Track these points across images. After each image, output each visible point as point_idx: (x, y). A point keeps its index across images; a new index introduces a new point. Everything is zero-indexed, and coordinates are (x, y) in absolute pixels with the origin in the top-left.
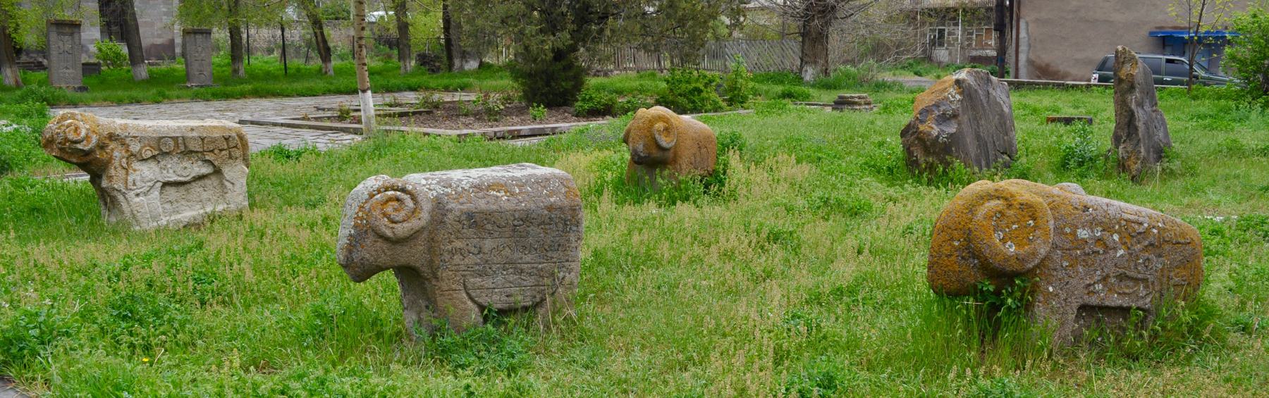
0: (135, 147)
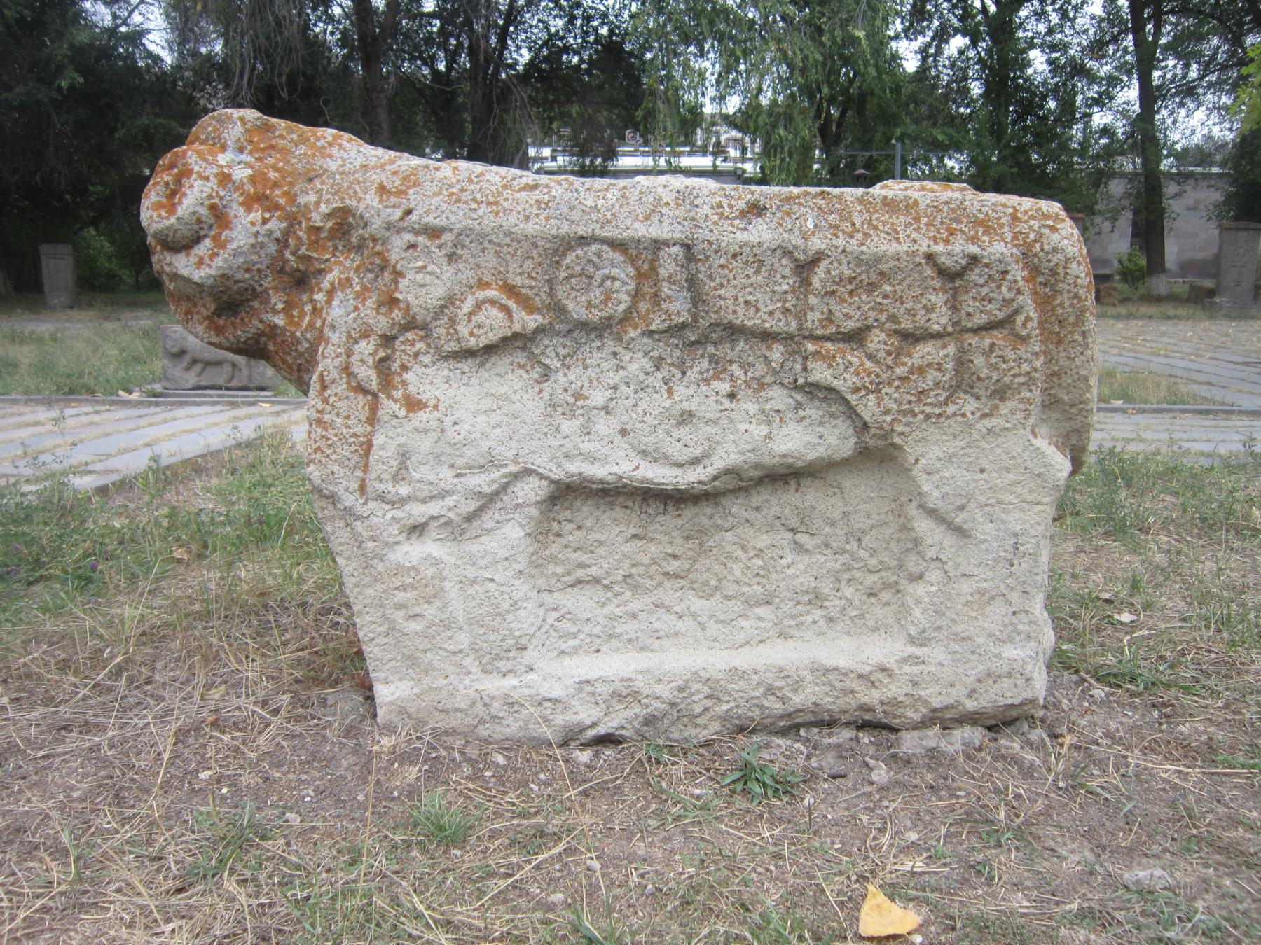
0: (425, 284)
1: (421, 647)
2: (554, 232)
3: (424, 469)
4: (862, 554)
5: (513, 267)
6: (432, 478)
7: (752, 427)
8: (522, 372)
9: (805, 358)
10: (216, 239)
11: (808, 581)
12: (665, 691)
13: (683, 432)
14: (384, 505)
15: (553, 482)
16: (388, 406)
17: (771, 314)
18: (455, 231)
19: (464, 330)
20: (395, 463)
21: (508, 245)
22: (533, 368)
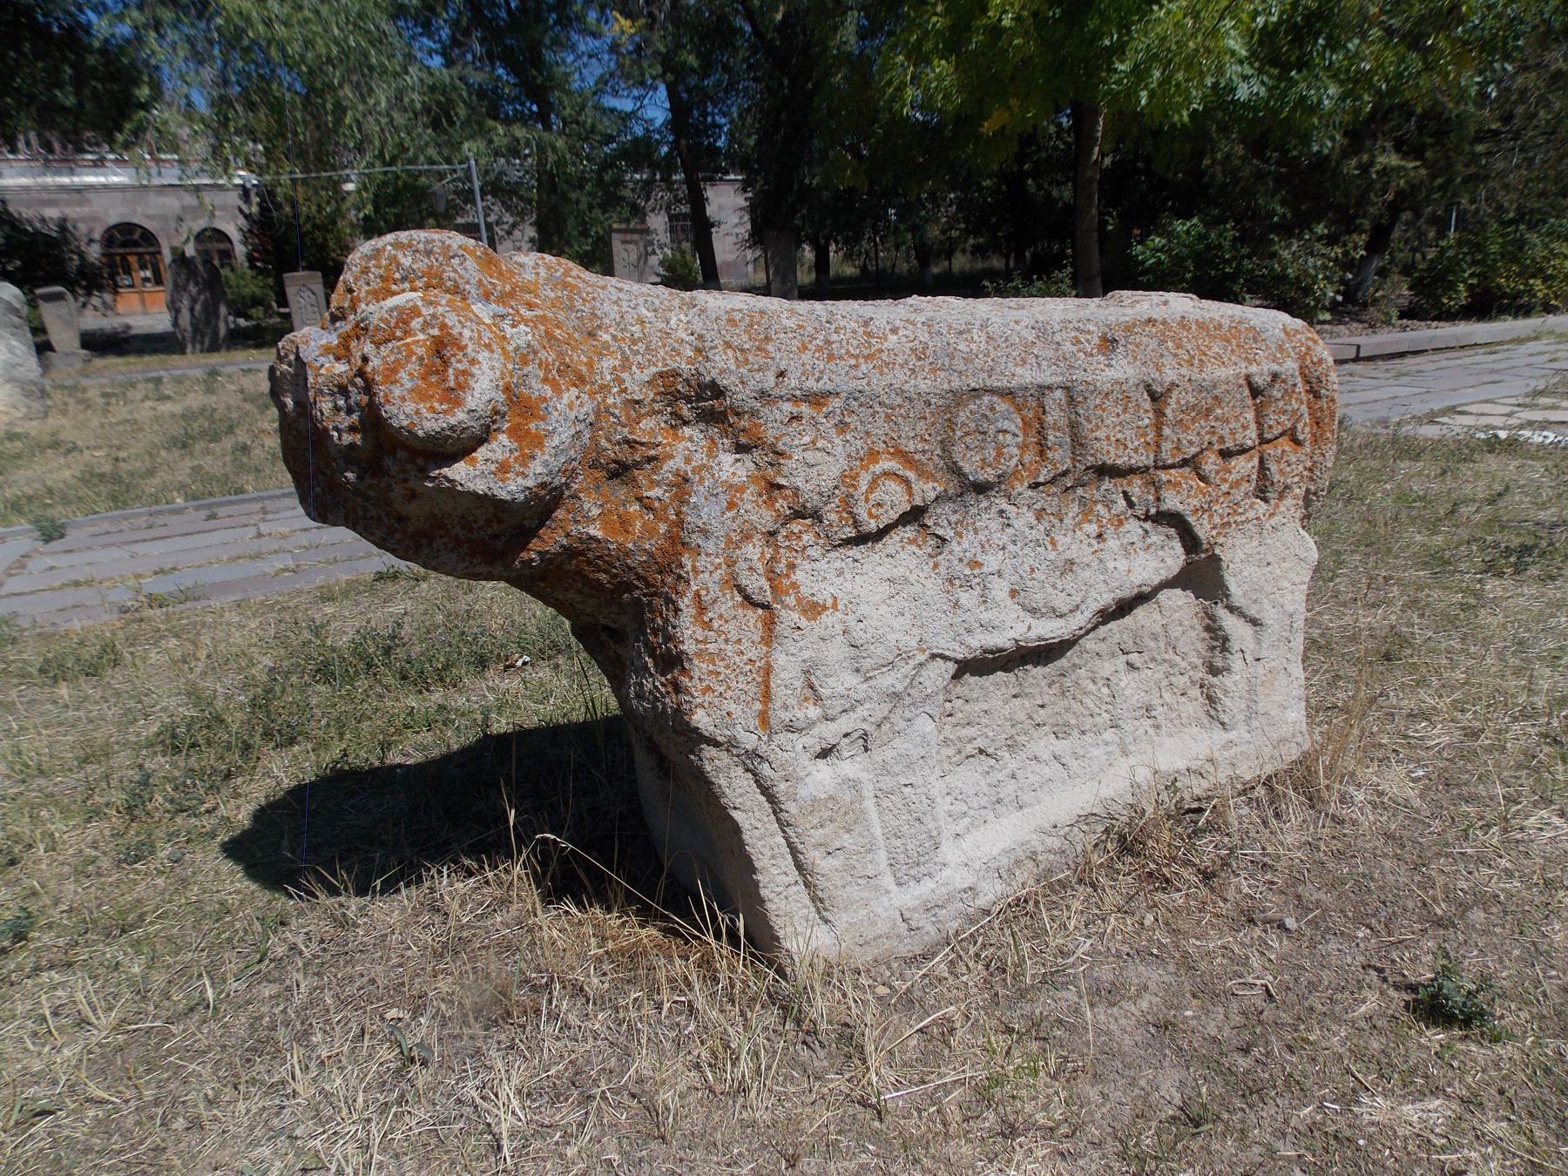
0: (816, 464)
1: (839, 883)
2: (946, 386)
3: (831, 681)
5: (906, 429)
6: (841, 690)
7: (1118, 564)
8: (914, 548)
9: (1158, 489)
10: (514, 433)
12: (1056, 843)
13: (1068, 583)
14: (790, 735)
15: (956, 662)
16: (789, 617)
17: (1136, 450)
18: (843, 395)
19: (862, 511)
20: (798, 684)
21: (900, 406)
22: (925, 542)
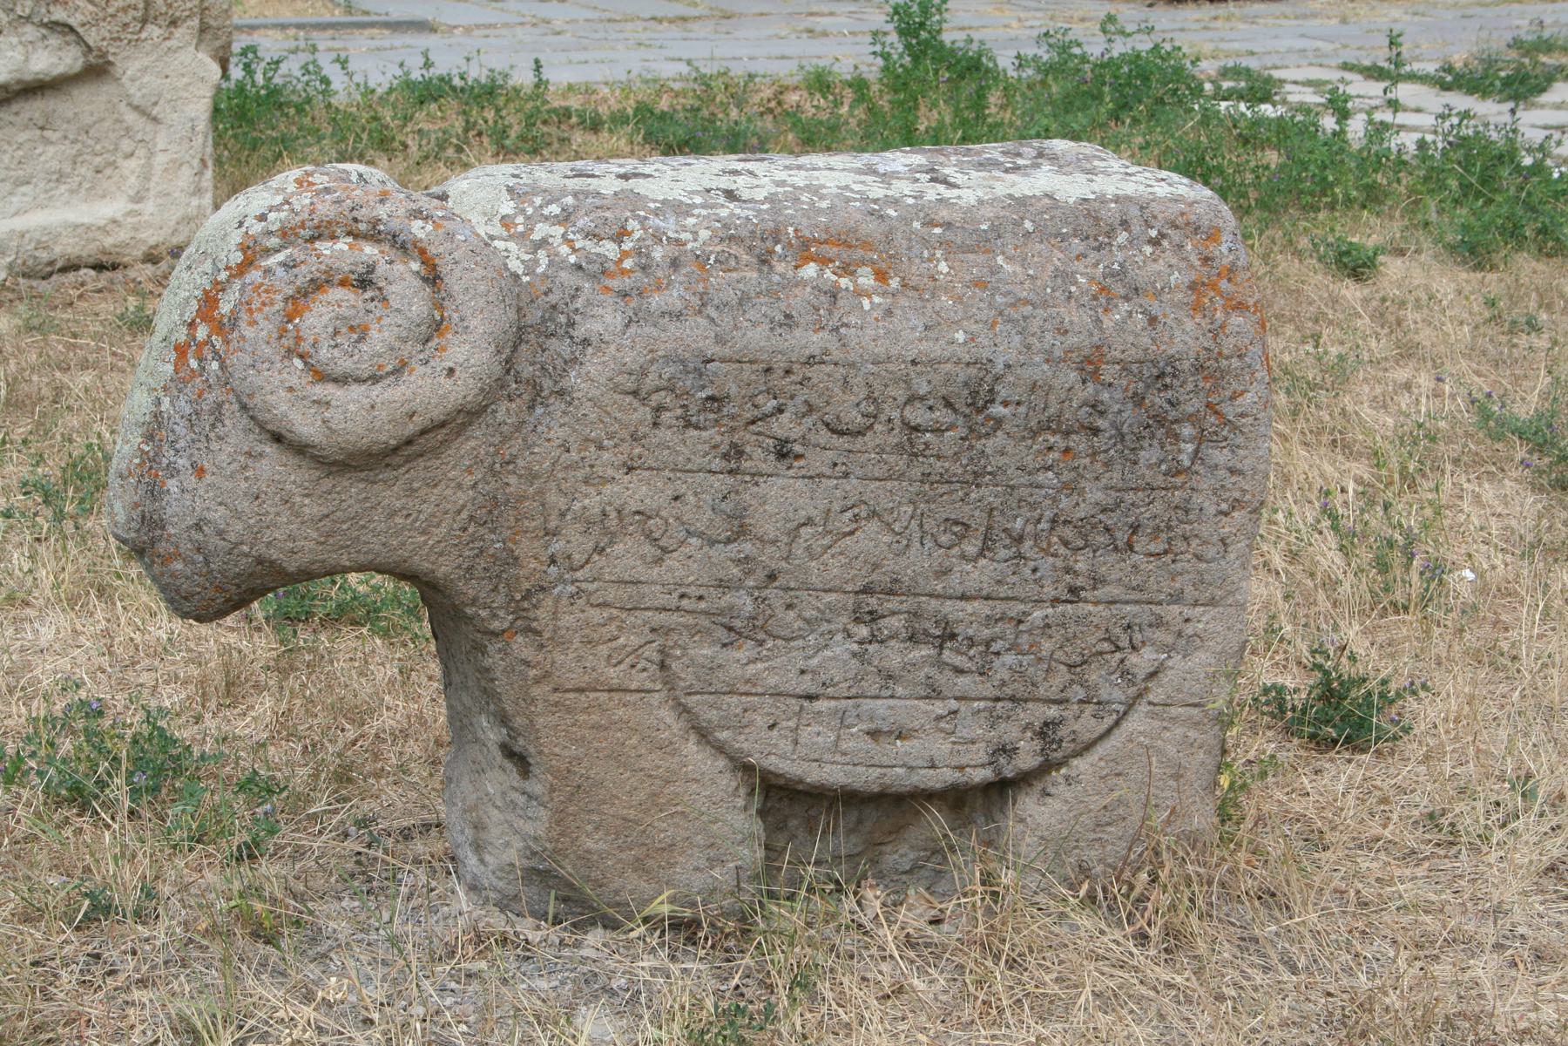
4: (90, 142)
11: (55, 165)
